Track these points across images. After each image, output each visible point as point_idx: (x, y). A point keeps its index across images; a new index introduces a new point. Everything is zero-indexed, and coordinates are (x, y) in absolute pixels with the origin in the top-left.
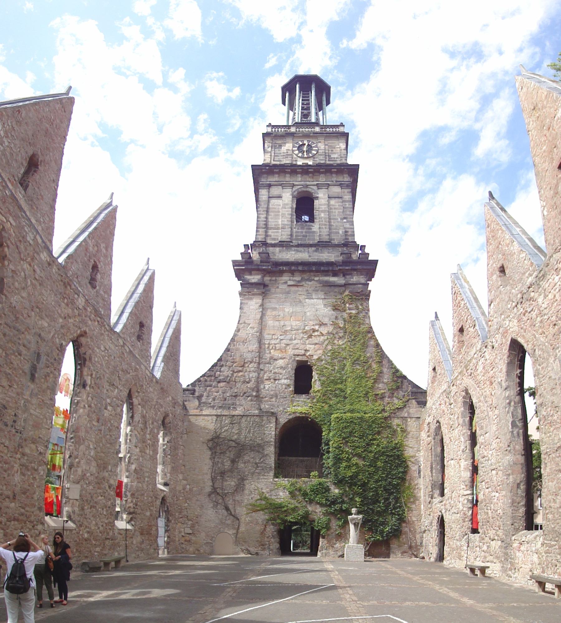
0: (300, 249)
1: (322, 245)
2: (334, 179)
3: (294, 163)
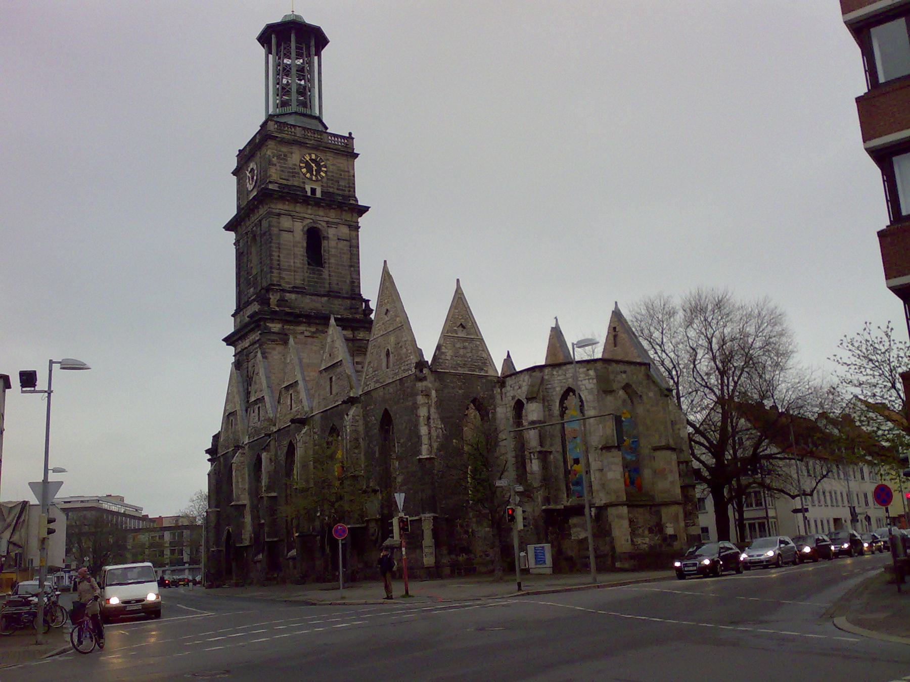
0: (313, 297)
1: (331, 294)
2: (343, 217)
3: (302, 185)
